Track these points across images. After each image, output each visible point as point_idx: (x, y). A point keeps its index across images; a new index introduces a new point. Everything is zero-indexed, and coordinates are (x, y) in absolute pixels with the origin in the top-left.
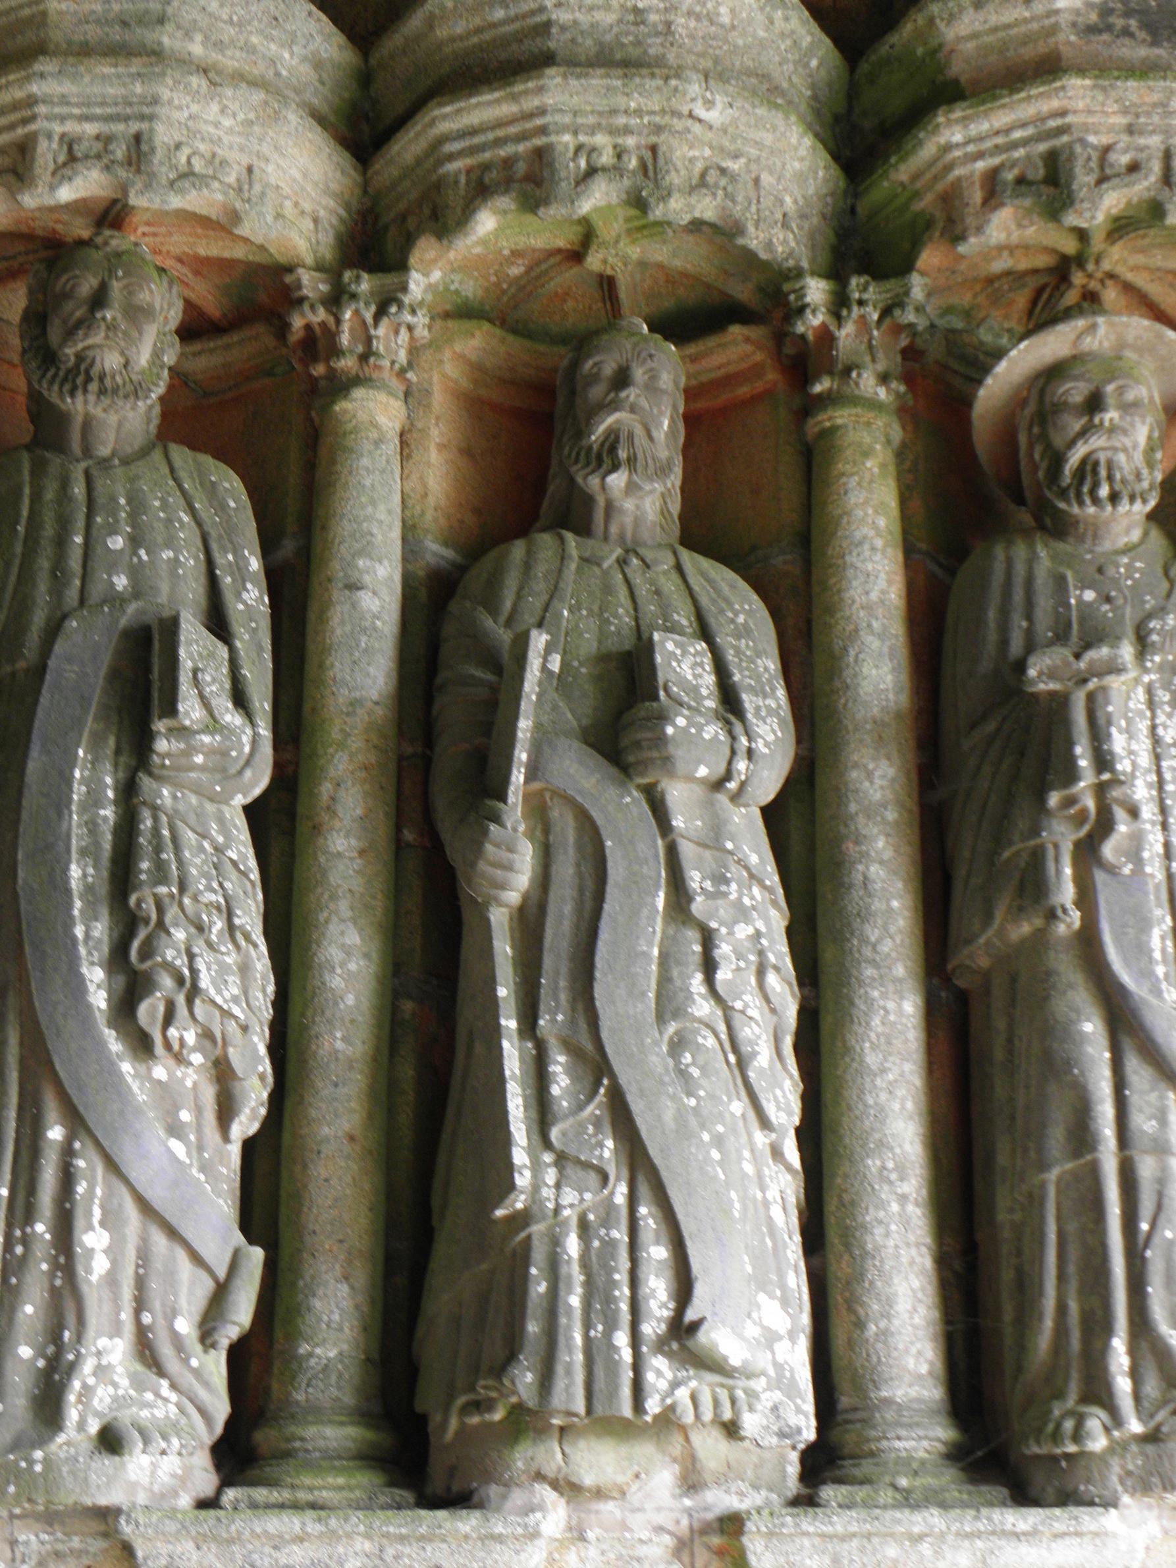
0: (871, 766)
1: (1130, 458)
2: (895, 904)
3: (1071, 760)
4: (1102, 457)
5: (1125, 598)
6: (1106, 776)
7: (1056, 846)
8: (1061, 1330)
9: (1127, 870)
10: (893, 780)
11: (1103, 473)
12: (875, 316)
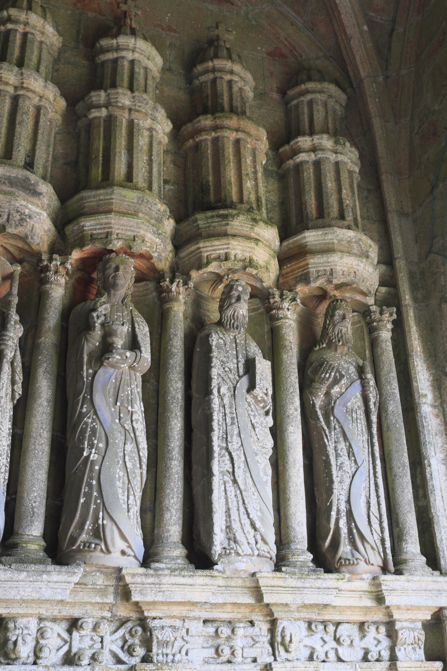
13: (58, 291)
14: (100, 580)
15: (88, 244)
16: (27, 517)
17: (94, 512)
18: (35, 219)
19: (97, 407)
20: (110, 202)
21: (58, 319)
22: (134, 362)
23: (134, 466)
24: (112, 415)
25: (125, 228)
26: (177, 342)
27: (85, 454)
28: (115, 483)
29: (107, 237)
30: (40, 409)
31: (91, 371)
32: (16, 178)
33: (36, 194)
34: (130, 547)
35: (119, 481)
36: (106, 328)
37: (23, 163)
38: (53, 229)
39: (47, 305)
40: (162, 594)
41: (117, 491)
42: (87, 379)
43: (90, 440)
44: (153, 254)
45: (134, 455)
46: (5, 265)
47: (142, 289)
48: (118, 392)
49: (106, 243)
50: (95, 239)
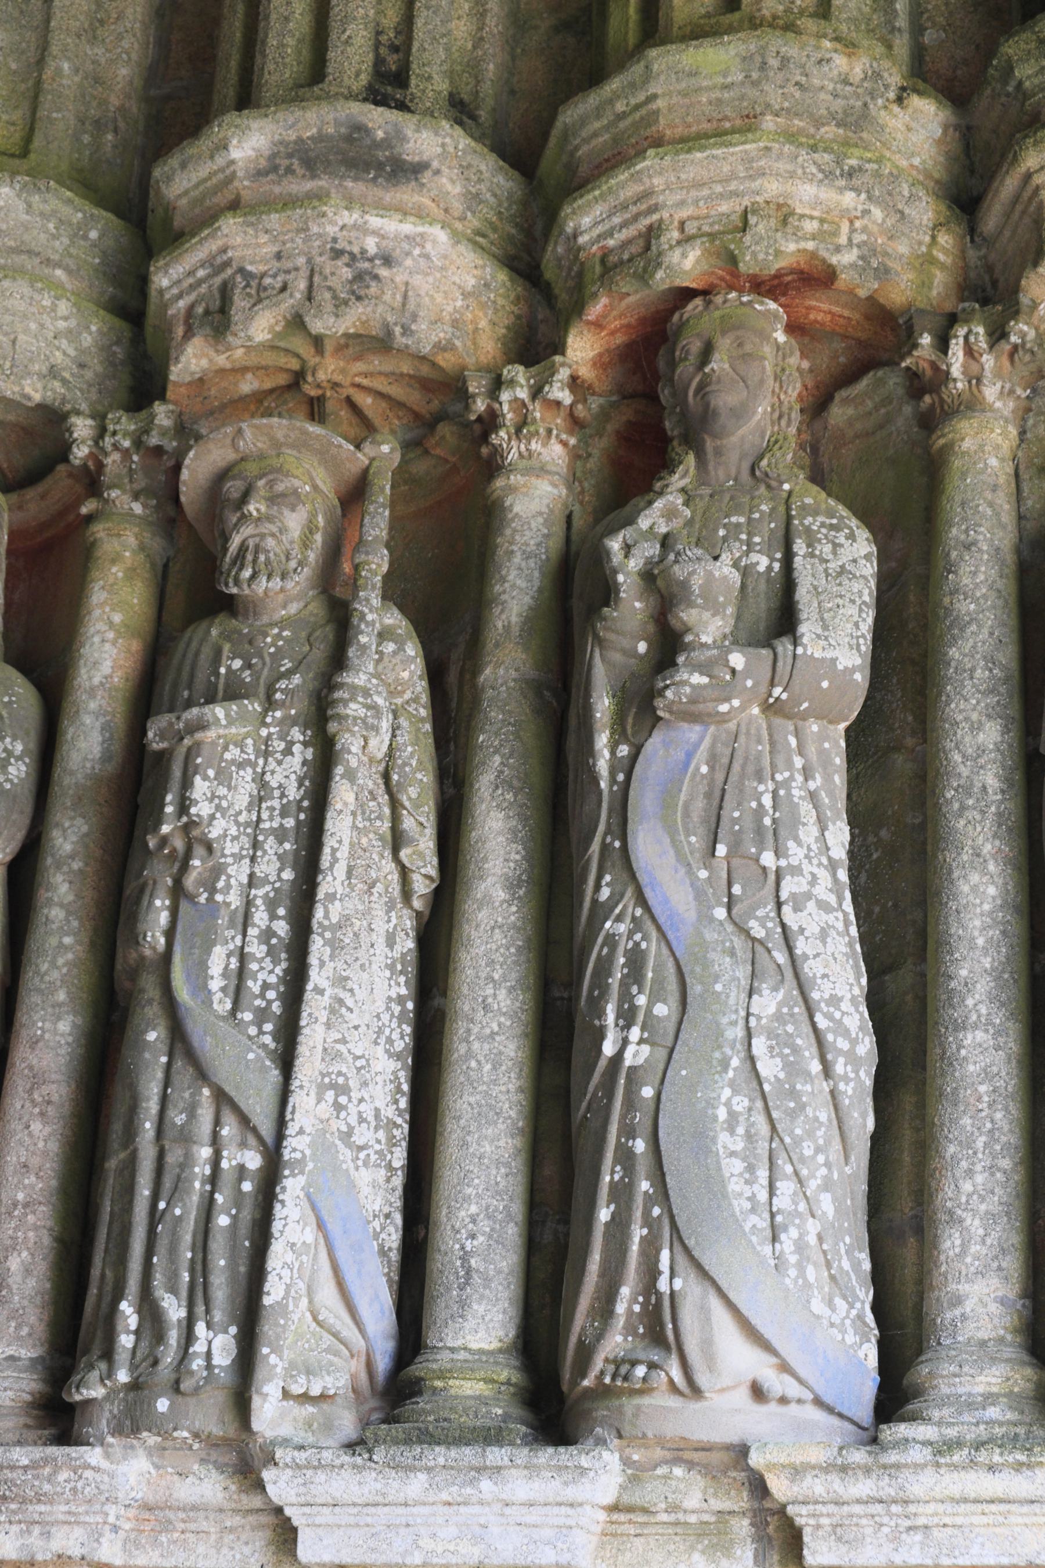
0: (67, 825)
1: (280, 542)
2: (67, 940)
3: (163, 805)
4: (251, 543)
5: (264, 664)
6: (185, 819)
7: (155, 882)
8: (100, 1296)
9: (202, 899)
10: (86, 835)
11: (249, 557)
12: (127, 444)
13: (538, 490)
14: (694, 1495)
15: (595, 295)
16: (449, 1289)
17: (643, 1253)
18: (409, 262)
19: (643, 878)
20: (649, 114)
21: (540, 590)
22: (772, 684)
23: (794, 1069)
24: (699, 895)
25: (706, 192)
26: (975, 573)
27: (608, 1048)
28: (714, 1141)
29: (648, 248)
30: (482, 915)
31: (624, 750)
32: (320, 138)
33: (402, 171)
34: (785, 1368)
35: (732, 1131)
36: (660, 582)
37: (364, 79)
38: (503, 276)
39: (500, 552)
40: (918, 1537)
41: (719, 1169)
42: (613, 780)
43: (626, 996)
44: (834, 260)
45: (790, 1029)
46: (334, 451)
47: (870, 404)
48: (721, 808)
49: (645, 270)
50: (616, 266)
